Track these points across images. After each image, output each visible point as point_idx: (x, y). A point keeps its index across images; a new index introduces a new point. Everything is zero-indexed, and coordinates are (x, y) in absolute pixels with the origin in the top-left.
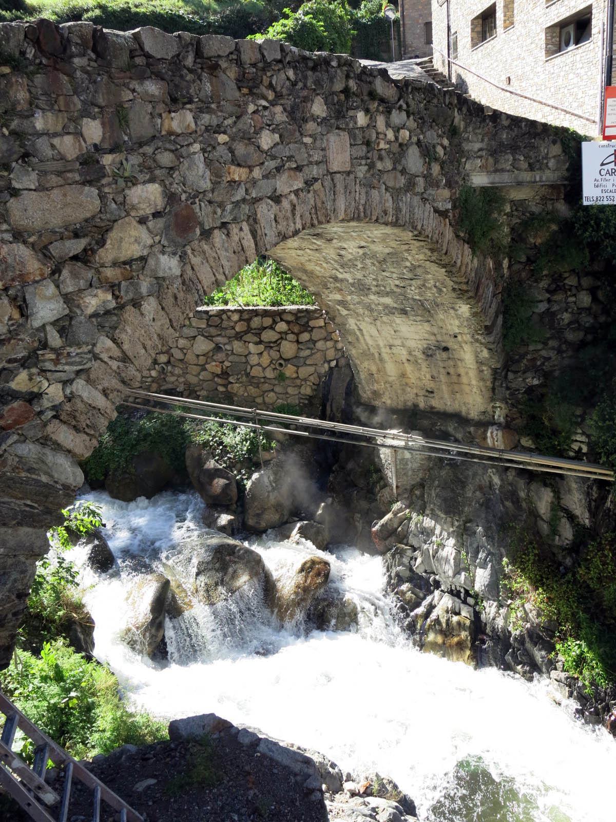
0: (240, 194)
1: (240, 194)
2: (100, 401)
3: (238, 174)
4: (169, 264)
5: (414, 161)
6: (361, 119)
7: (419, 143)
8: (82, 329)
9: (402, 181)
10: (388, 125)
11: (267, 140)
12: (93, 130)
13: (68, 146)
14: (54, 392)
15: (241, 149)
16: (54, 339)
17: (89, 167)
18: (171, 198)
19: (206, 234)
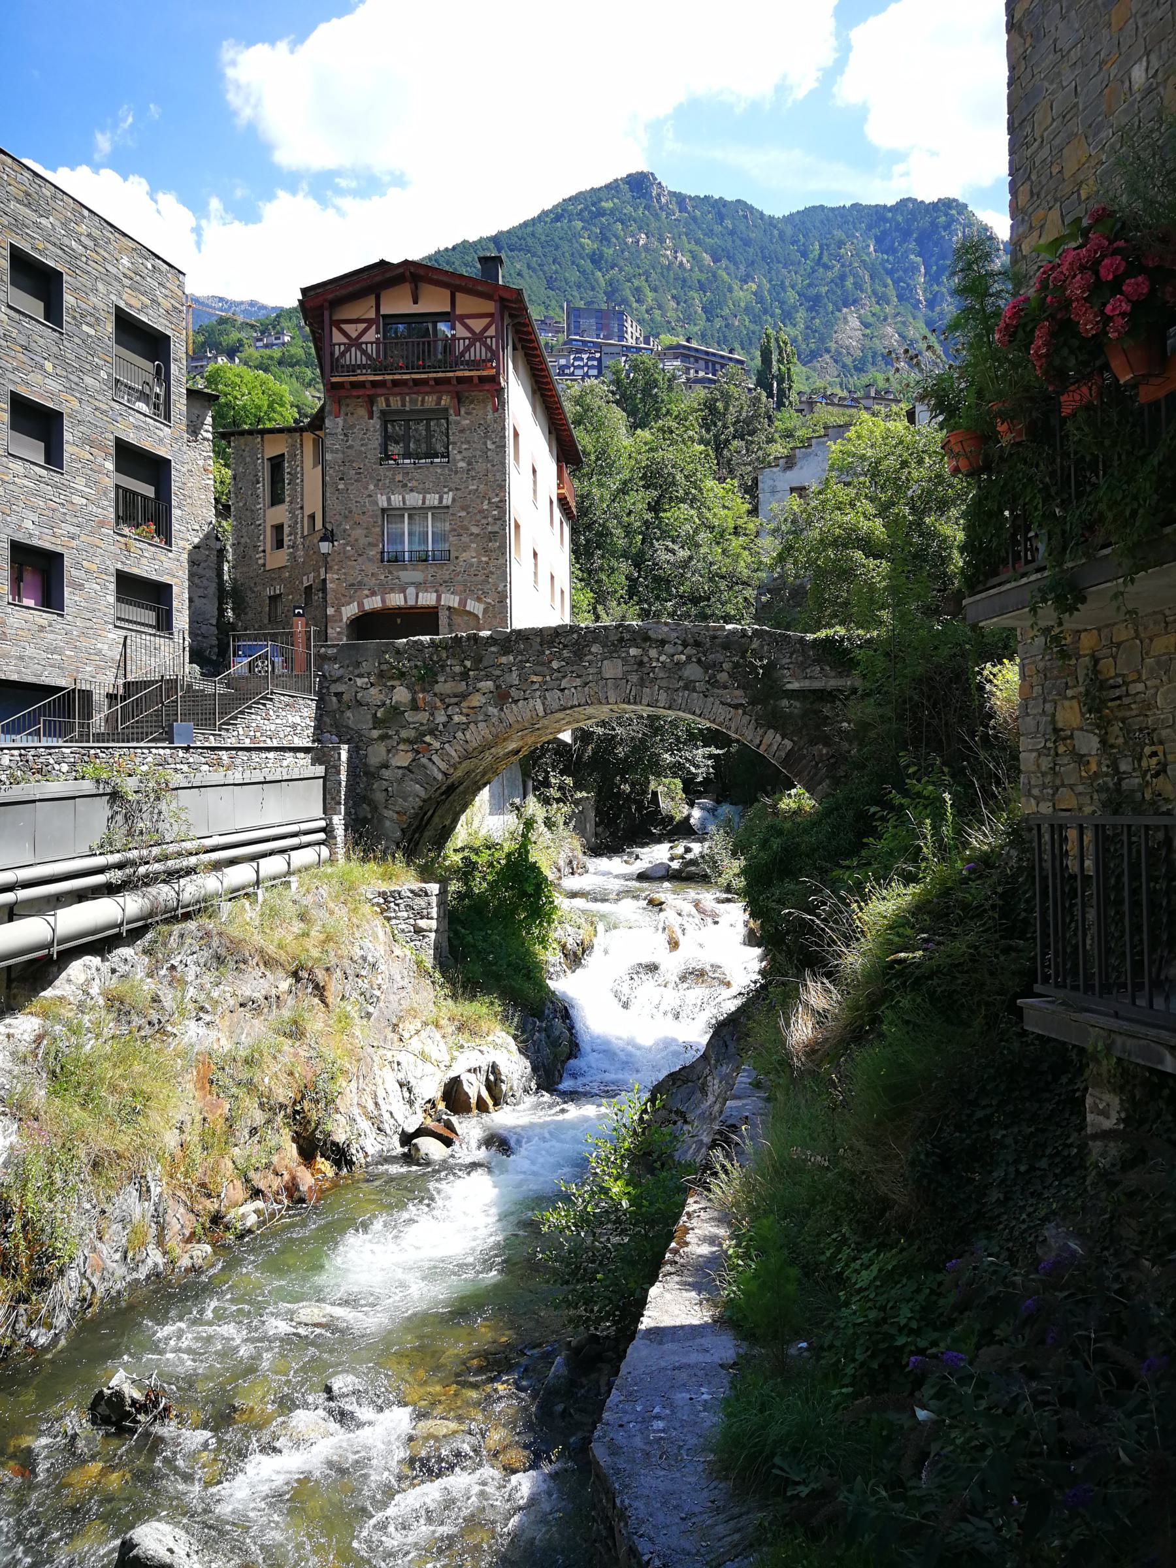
0: (536, 686)
1: (536, 686)
2: (454, 754)
3: (535, 679)
4: (492, 710)
5: (693, 672)
6: (633, 651)
7: (699, 661)
8: (451, 729)
9: (681, 683)
10: (660, 654)
11: (555, 665)
12: (468, 664)
13: (457, 669)
14: (437, 745)
15: (538, 669)
16: (441, 727)
17: (464, 676)
18: (498, 687)
19: (516, 702)
